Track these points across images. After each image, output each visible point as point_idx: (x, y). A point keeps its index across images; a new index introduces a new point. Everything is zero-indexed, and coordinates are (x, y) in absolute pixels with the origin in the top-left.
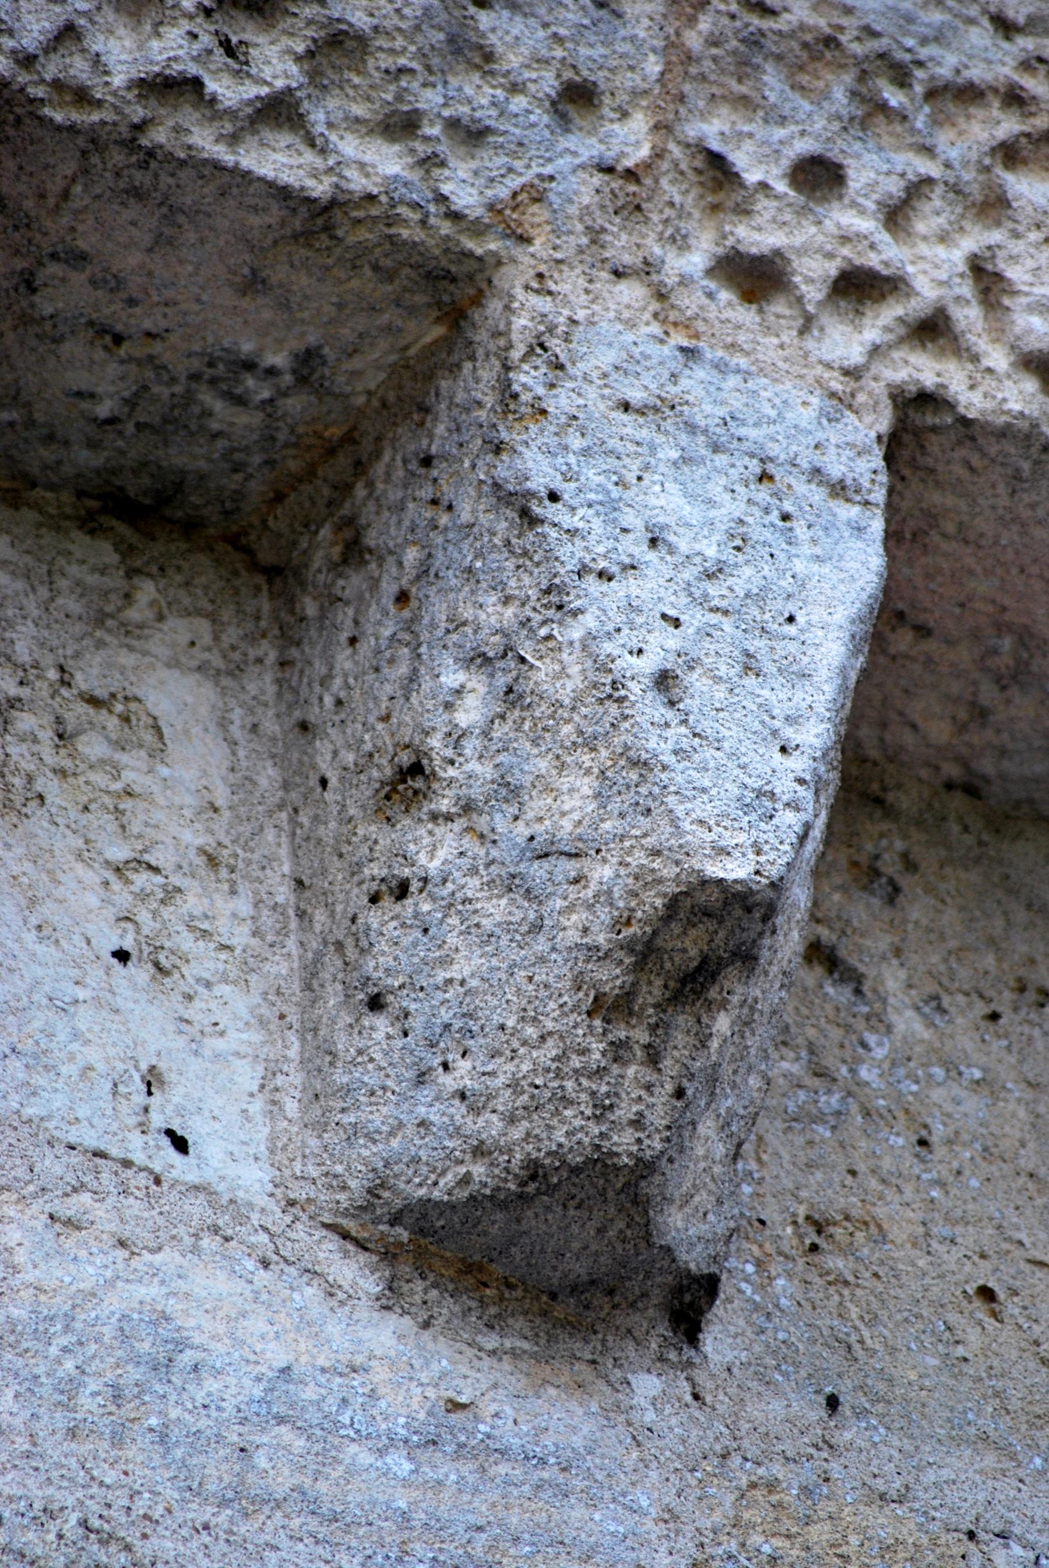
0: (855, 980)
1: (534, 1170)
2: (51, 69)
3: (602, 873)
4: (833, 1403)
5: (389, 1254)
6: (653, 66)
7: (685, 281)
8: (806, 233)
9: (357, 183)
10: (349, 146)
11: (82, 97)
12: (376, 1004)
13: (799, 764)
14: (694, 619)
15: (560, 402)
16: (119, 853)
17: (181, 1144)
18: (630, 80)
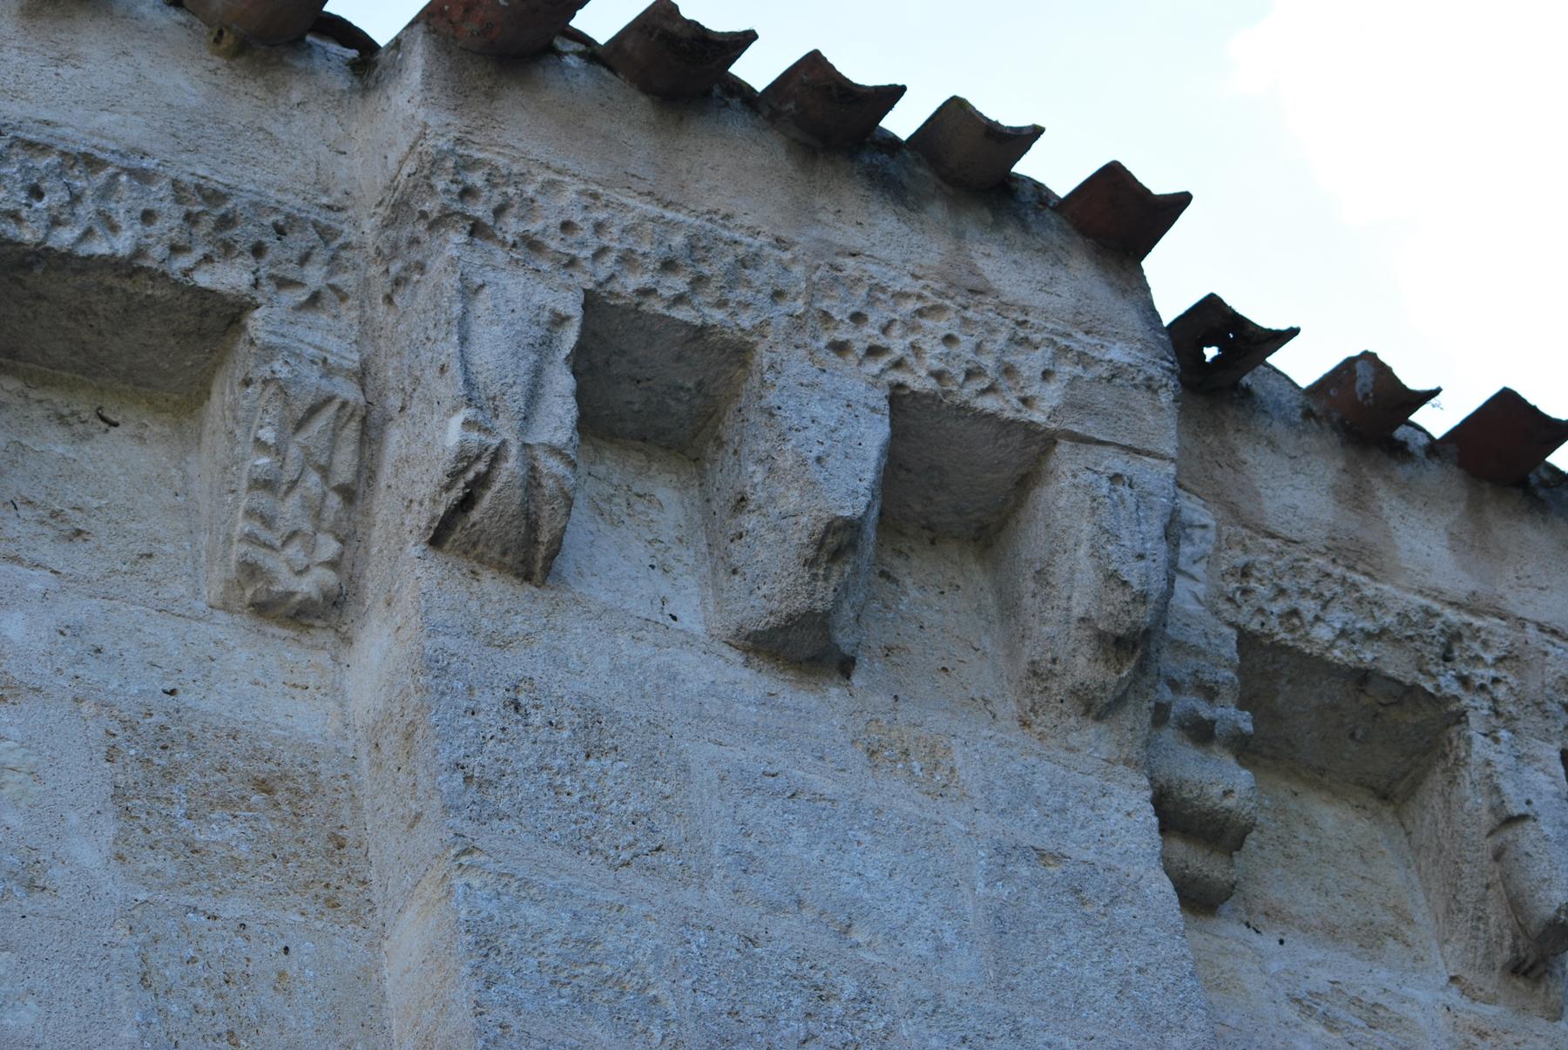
0: (895, 581)
1: (790, 617)
2: (609, 288)
3: (804, 520)
4: (896, 698)
5: (746, 651)
6: (803, 285)
7: (819, 349)
8: (857, 335)
9: (710, 322)
10: (706, 310)
11: (618, 296)
12: (735, 572)
13: (865, 484)
14: (828, 443)
15: (780, 382)
16: (650, 537)
17: (674, 618)
18: (794, 290)
